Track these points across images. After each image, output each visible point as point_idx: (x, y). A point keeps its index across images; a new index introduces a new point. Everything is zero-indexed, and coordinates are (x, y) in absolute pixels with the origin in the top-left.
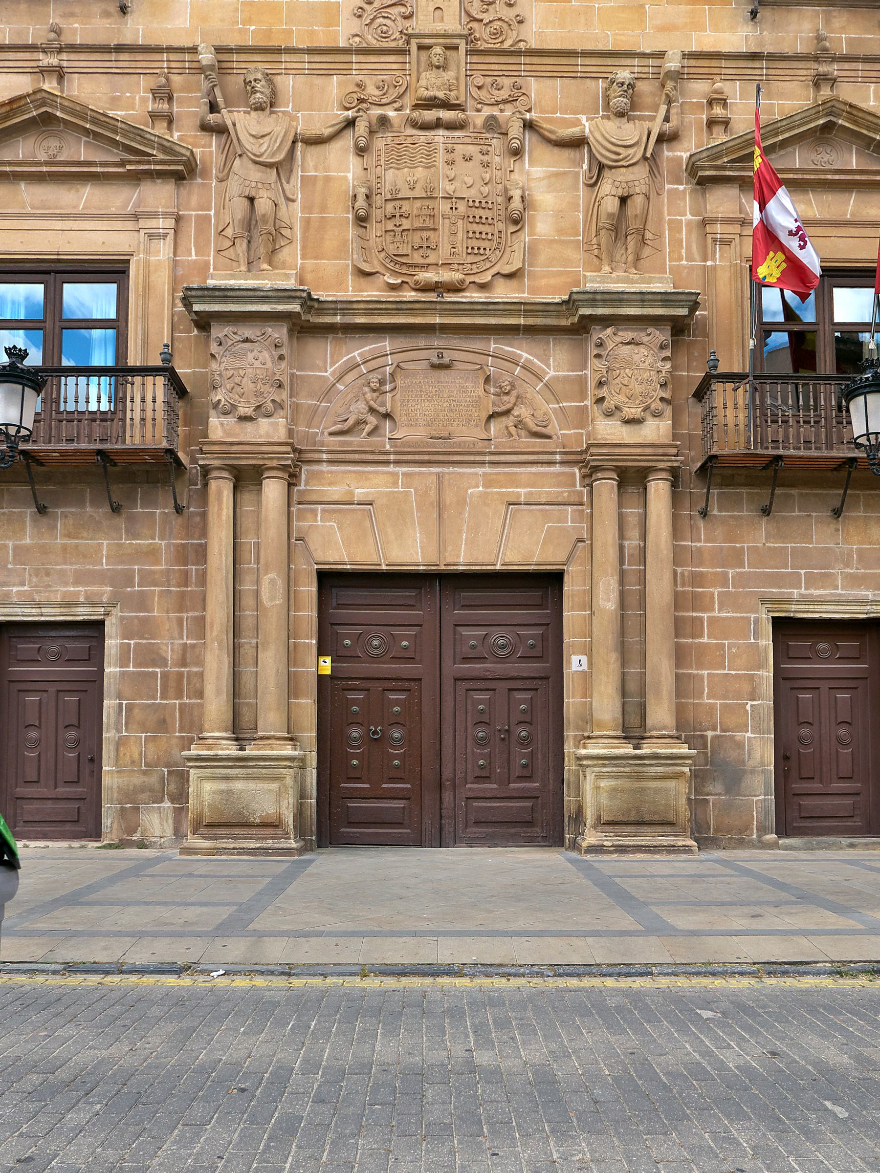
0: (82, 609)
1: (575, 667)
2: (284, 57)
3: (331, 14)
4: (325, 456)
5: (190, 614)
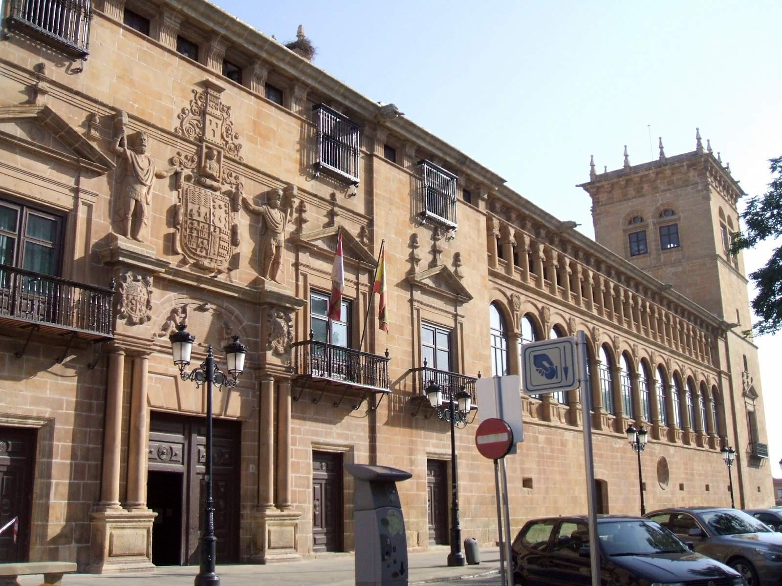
0: (31, 421)
1: (251, 470)
2: (150, 128)
3: (169, 112)
4: (158, 348)
5: (92, 429)
